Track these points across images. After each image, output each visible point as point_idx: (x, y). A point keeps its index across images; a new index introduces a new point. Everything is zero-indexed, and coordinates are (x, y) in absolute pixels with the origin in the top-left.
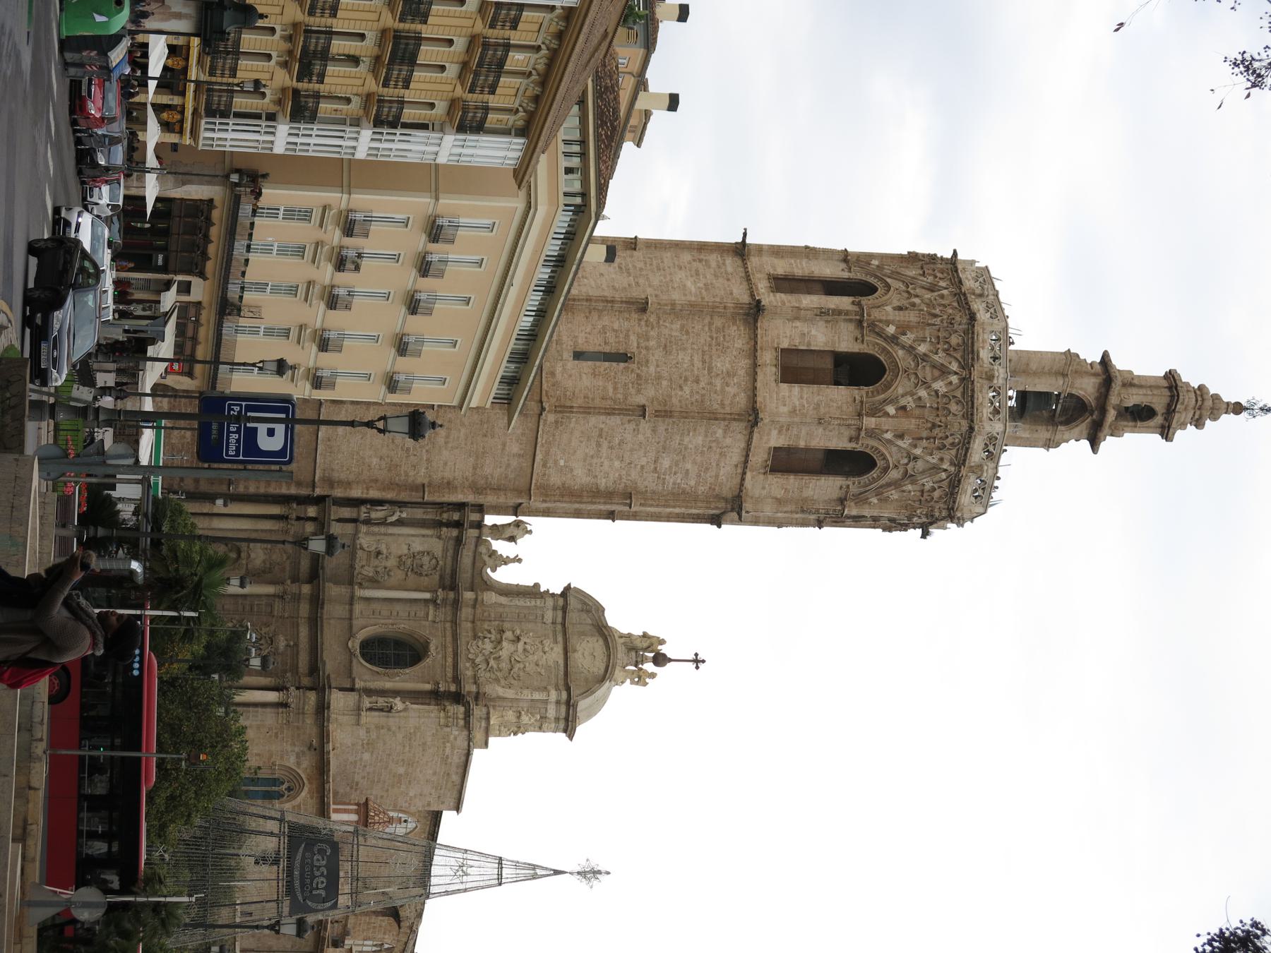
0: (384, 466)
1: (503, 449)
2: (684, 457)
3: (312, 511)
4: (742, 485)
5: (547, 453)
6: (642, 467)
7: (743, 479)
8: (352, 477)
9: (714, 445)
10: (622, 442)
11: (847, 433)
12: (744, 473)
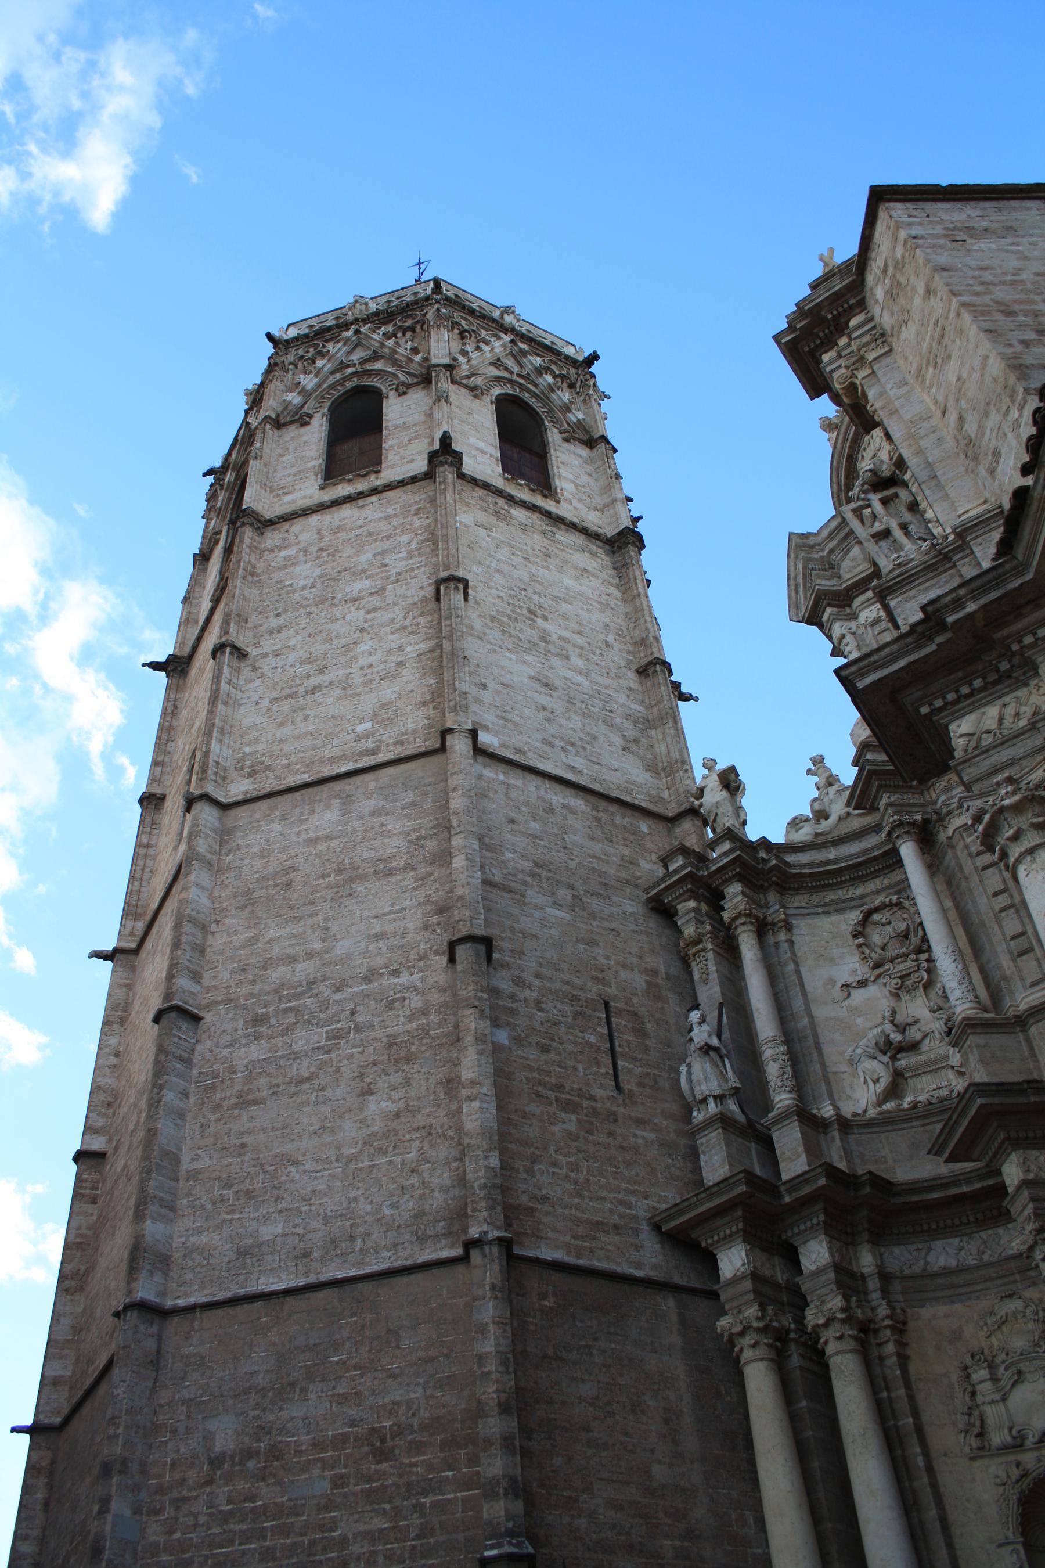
0: (396, 1078)
1: (329, 838)
2: (345, 570)
3: (733, 1261)
4: (401, 484)
5: (332, 760)
6: (369, 612)
7: (389, 487)
8: (443, 1151)
9: (314, 549)
10: (309, 661)
11: (292, 431)
12: (374, 491)
